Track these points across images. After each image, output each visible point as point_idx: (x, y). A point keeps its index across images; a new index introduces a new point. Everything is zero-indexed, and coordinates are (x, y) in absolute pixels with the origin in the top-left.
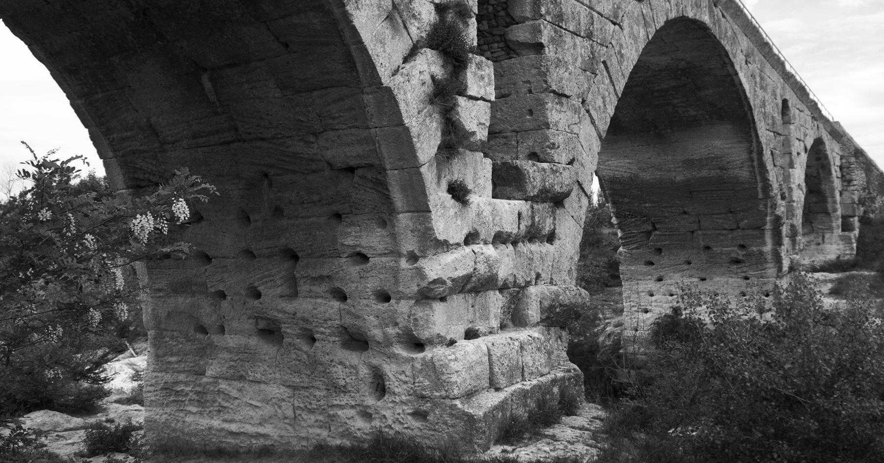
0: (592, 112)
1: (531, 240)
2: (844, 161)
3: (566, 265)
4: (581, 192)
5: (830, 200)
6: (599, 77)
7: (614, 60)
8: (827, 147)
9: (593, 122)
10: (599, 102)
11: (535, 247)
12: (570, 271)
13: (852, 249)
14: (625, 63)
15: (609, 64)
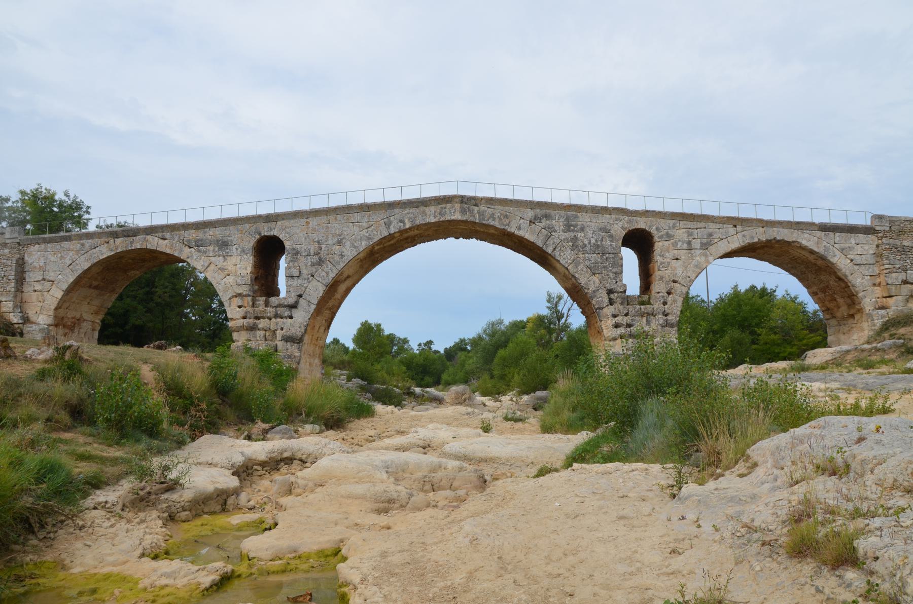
0: (317, 278)
1: (282, 318)
2: (880, 248)
3: (298, 325)
4: (310, 304)
5: (849, 284)
6: (325, 266)
7: (337, 258)
8: (804, 243)
9: (319, 281)
10: (324, 274)
11: (285, 320)
12: (300, 327)
13: (874, 325)
14: (346, 257)
15: (331, 260)
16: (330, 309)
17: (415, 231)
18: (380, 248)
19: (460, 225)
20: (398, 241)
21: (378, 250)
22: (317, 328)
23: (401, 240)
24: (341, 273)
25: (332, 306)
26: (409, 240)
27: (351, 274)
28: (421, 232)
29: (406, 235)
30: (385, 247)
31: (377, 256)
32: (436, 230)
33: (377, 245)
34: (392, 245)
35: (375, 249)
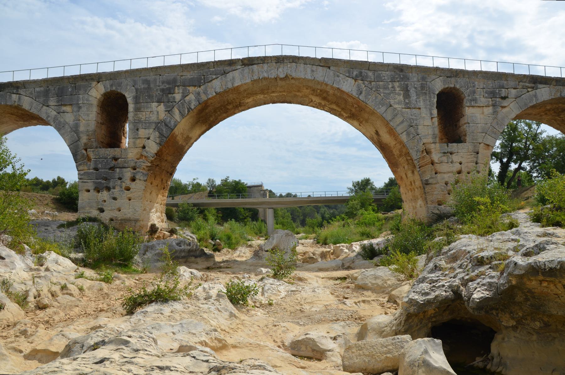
16: (401, 155)
17: (314, 100)
18: (345, 112)
19: (276, 96)
20: (332, 103)
21: (346, 113)
22: (404, 176)
23: (328, 101)
24: (371, 139)
25: (400, 152)
26: (325, 95)
27: (374, 130)
28: (311, 96)
29: (323, 103)
30: (343, 109)
31: (353, 110)
32: (299, 91)
33: (343, 116)
34: (338, 105)
35: (347, 115)
